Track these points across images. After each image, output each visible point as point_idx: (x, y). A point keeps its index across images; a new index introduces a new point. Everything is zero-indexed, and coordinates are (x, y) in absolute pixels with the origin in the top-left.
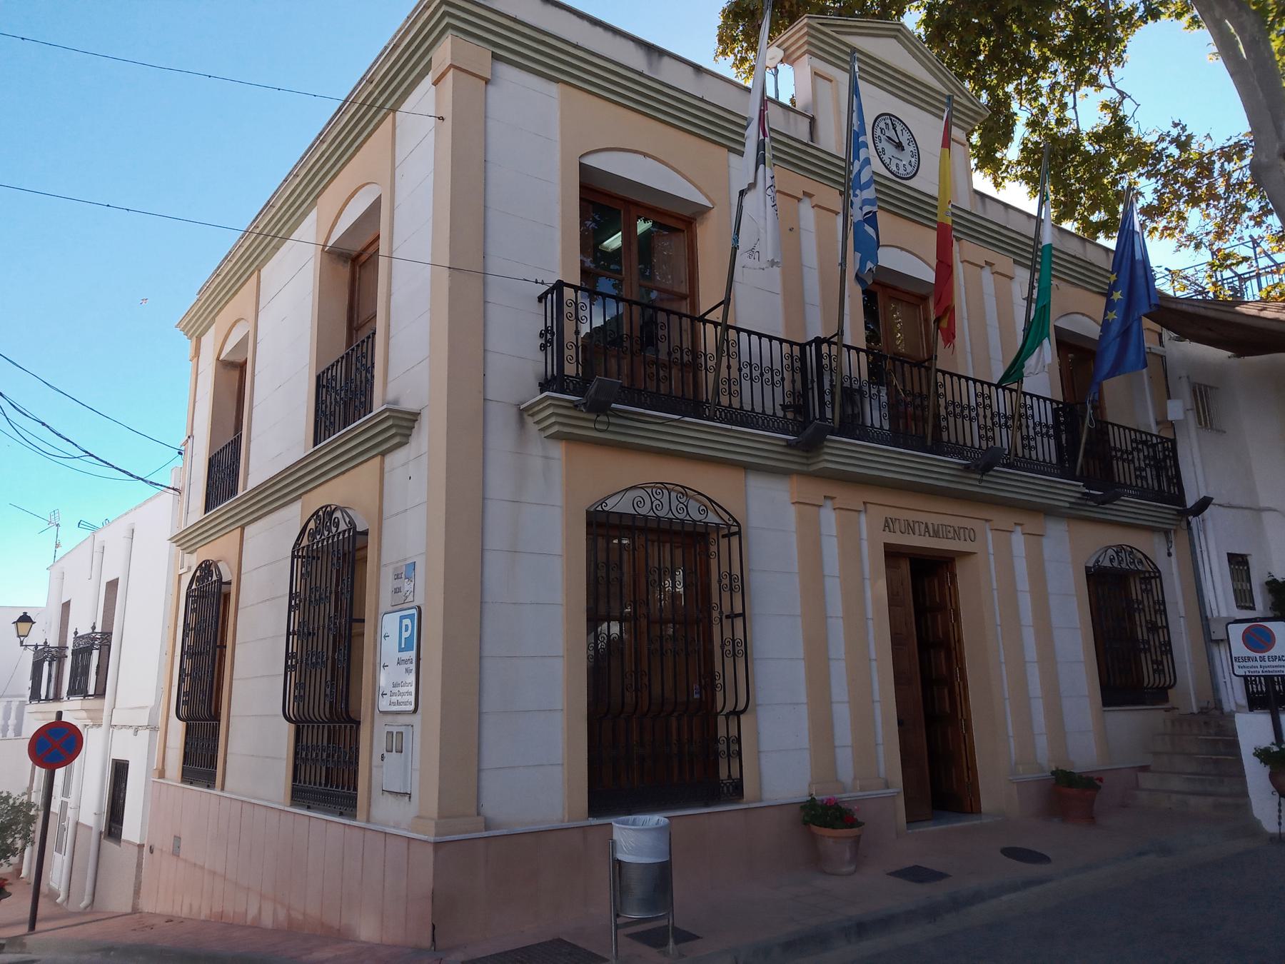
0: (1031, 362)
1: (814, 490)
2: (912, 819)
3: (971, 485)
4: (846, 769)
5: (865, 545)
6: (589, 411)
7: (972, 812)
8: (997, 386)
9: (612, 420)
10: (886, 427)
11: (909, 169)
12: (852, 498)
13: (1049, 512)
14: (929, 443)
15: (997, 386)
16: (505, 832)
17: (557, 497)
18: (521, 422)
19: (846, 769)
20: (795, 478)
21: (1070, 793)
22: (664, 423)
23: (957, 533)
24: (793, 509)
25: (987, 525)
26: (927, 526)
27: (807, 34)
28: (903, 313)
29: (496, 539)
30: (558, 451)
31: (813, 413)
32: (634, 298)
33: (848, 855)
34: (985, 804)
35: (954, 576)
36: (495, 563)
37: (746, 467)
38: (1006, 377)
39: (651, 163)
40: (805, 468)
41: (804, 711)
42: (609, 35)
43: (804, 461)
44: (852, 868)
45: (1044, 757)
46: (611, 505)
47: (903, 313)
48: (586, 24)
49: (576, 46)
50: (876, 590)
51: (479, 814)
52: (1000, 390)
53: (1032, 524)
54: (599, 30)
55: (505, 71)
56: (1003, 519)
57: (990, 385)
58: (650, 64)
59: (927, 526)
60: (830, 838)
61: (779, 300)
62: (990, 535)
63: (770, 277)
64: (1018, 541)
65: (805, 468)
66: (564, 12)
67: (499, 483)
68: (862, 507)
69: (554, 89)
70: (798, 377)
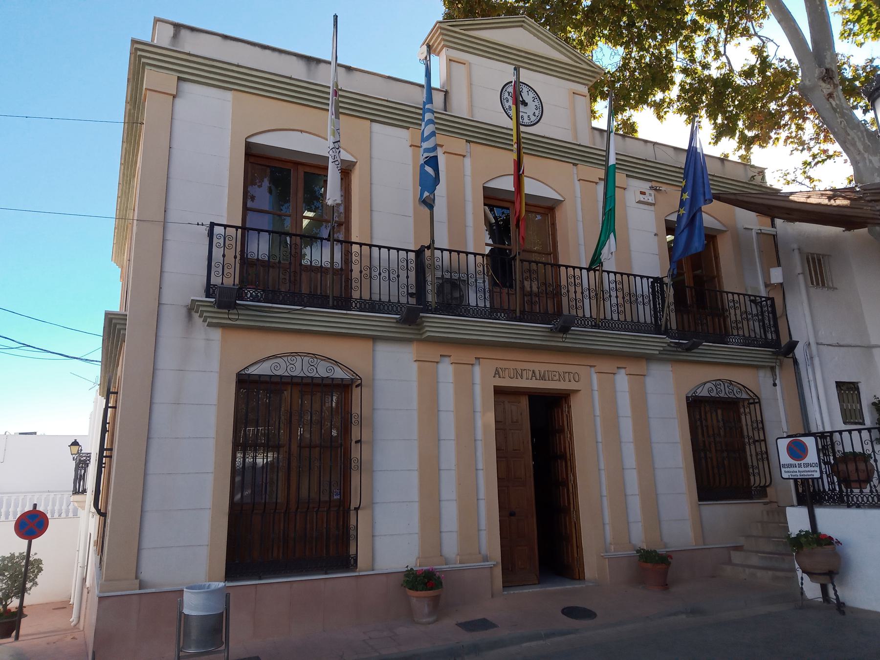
0: (605, 251)
1: (431, 352)
2: (509, 582)
3: (558, 341)
4: (451, 547)
5: (478, 389)
6: (219, 307)
7: (579, 579)
8: (588, 270)
9: (240, 312)
10: (488, 305)
11: (533, 118)
12: (467, 355)
13: (648, 358)
14: (518, 315)
15: (588, 270)
16: (153, 590)
17: (215, 366)
18: (190, 316)
19: (451, 547)
20: (415, 343)
21: (653, 566)
22: (290, 311)
23: (561, 378)
24: (416, 365)
25: (593, 369)
26: (534, 372)
27: (441, 34)
28: (514, 220)
29: (163, 395)
30: (216, 334)
31: (428, 299)
32: (271, 229)
33: (426, 610)
34: (588, 573)
35: (569, 407)
36: (161, 412)
37: (374, 339)
38: (593, 262)
39: (300, 135)
40: (419, 337)
41: (416, 507)
42: (276, 54)
43: (416, 332)
44: (431, 619)
45: (639, 537)
46: (254, 371)
47: (514, 220)
48: (257, 49)
49: (238, 66)
50: (485, 420)
51: (137, 578)
52: (592, 273)
53: (634, 368)
54: (268, 52)
55: (187, 87)
56: (606, 365)
57: (581, 269)
58: (309, 70)
59: (534, 372)
60: (419, 600)
61: (411, 221)
62: (595, 377)
63: (388, 209)
64: (622, 381)
65: (419, 337)
66: (240, 43)
67: (167, 359)
68: (473, 361)
69: (229, 95)
70: (412, 275)
